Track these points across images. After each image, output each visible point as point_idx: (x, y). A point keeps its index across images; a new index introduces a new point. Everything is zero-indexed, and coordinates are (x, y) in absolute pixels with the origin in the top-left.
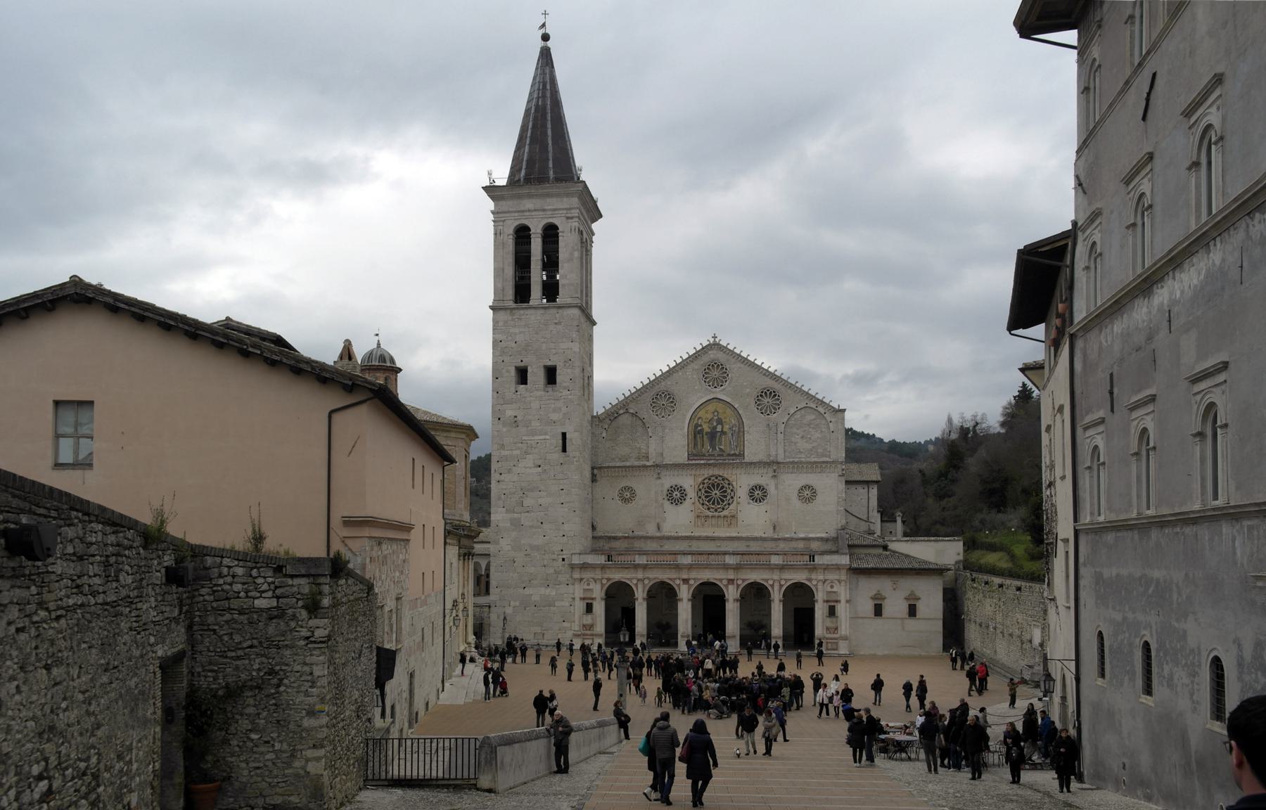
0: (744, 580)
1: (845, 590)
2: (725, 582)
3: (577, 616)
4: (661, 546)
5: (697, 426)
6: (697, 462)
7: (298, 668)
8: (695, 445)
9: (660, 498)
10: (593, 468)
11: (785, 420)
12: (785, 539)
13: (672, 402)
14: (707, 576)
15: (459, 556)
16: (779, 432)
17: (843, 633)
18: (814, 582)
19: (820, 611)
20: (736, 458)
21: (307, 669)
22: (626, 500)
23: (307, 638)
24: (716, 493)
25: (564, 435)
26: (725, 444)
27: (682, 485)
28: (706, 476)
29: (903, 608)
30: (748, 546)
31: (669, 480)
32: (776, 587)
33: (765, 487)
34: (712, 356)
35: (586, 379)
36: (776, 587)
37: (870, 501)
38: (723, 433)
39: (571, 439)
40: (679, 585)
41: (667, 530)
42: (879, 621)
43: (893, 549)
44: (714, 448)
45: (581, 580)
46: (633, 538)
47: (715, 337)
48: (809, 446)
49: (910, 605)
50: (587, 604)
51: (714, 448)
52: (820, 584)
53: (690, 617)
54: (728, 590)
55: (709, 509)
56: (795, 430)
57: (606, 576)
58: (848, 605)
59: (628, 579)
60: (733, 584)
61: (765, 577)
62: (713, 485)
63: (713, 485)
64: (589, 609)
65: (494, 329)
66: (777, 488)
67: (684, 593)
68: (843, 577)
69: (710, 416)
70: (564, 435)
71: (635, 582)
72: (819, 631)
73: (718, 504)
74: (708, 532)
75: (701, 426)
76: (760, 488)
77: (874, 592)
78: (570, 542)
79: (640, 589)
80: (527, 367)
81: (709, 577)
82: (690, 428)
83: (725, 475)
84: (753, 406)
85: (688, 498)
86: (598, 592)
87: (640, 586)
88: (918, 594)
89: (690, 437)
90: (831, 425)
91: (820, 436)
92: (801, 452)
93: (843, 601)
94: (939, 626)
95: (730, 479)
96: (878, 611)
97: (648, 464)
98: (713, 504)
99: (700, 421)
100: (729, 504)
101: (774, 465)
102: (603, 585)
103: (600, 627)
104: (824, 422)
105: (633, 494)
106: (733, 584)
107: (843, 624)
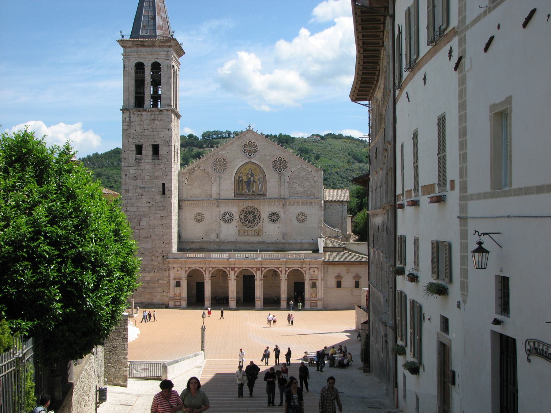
0: (265, 268)
1: (321, 274)
2: (255, 269)
4: (219, 247)
5: (239, 177)
8: (239, 188)
9: (218, 219)
11: (289, 175)
17: (320, 297)
19: (307, 287)
20: (263, 196)
21: (123, 346)
23: (123, 337)
24: (250, 217)
25: (163, 184)
26: (256, 188)
27: (231, 211)
28: (245, 206)
29: (352, 283)
32: (283, 272)
33: (278, 213)
34: (248, 137)
35: (176, 150)
36: (283, 272)
37: (343, 213)
38: (254, 181)
40: (229, 271)
42: (339, 290)
43: (349, 248)
44: (249, 191)
45: (174, 268)
47: (250, 126)
48: (302, 190)
49: (355, 281)
50: (177, 281)
51: (249, 191)
53: (235, 289)
55: (246, 226)
56: (295, 181)
58: (322, 281)
60: (259, 270)
62: (249, 212)
63: (249, 212)
64: (178, 284)
65: (123, 123)
66: (285, 214)
67: (232, 276)
69: (247, 172)
70: (163, 184)
71: (204, 269)
72: (307, 295)
73: (252, 222)
74: (246, 239)
75: (242, 177)
76: (275, 213)
78: (167, 246)
81: (246, 266)
82: (236, 179)
84: (271, 167)
85: (234, 220)
86: (183, 275)
87: (207, 272)
88: (360, 275)
89: (236, 184)
90: (315, 178)
92: (298, 193)
95: (258, 208)
96: (339, 285)
99: (241, 175)
100: (258, 223)
102: (186, 271)
103: (185, 294)
104: (311, 176)
107: (320, 292)
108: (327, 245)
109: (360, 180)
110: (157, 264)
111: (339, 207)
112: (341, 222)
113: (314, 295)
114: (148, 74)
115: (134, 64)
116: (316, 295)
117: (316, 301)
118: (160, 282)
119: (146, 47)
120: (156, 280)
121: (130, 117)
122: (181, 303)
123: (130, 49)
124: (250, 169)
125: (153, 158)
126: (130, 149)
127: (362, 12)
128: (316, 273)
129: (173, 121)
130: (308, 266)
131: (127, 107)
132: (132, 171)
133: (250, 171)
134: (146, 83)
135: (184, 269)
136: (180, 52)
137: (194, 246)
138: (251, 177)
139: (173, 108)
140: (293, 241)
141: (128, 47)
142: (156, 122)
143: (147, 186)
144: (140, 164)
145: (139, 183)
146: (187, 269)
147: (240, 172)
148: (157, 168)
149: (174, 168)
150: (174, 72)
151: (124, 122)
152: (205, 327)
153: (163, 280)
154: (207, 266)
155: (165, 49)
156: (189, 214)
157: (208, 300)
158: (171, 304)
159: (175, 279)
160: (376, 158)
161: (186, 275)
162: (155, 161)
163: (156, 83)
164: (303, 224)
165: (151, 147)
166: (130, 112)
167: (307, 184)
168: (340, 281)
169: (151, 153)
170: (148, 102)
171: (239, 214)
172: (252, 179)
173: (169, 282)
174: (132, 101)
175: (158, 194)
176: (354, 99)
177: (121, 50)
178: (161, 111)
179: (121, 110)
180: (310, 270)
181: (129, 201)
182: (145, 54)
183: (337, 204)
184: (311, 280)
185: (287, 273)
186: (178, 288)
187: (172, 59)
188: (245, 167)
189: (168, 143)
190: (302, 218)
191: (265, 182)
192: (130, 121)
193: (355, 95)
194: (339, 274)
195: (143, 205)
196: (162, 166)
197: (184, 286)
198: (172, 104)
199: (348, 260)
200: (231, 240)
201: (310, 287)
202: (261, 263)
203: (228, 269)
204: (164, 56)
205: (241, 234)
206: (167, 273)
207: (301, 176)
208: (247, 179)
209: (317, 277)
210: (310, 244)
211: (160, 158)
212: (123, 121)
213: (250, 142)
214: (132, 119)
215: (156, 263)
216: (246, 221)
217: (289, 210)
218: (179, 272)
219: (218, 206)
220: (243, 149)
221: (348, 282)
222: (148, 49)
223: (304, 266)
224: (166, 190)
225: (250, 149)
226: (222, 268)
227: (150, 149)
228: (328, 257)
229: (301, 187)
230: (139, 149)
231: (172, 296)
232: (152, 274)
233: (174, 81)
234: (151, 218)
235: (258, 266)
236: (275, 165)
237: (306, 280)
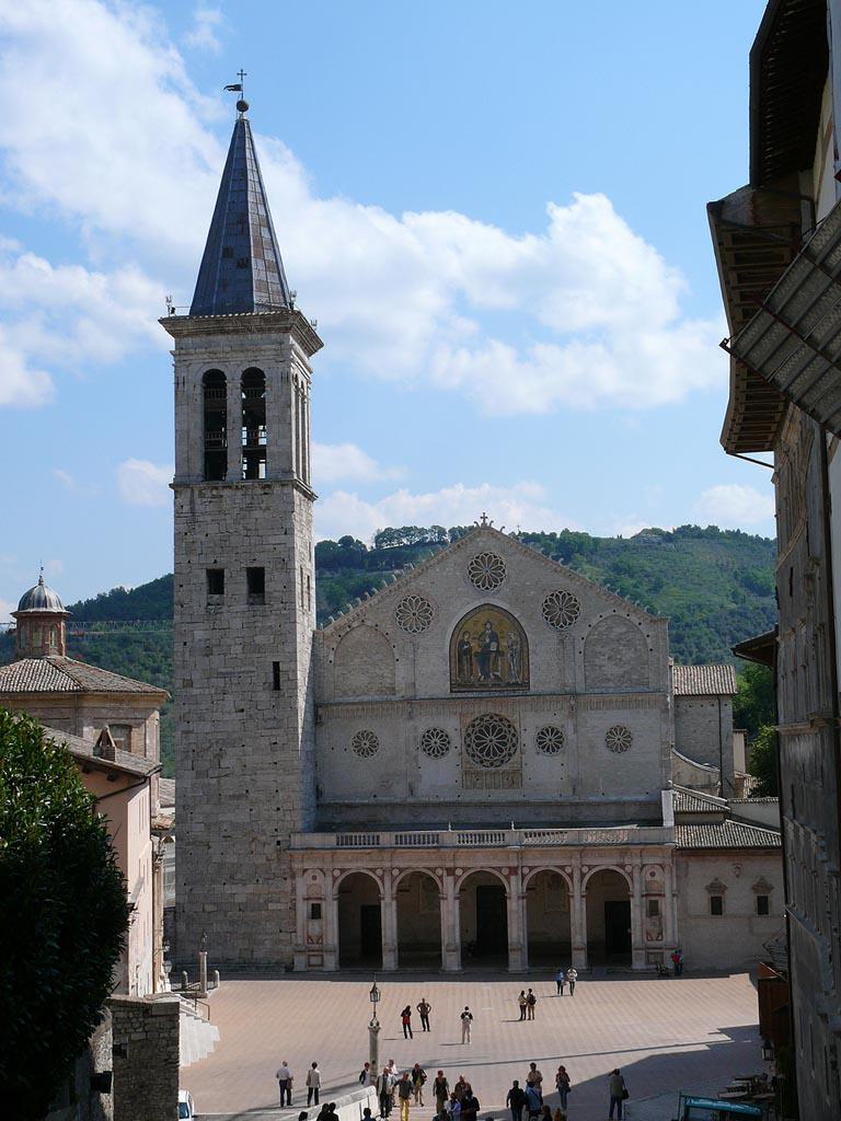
0: (531, 868)
1: (671, 878)
2: (505, 872)
5: (462, 643)
6: (464, 695)
7: (160, 1081)
8: (461, 670)
12: (590, 804)
13: (427, 611)
14: (481, 862)
16: (577, 653)
19: (637, 913)
22: (364, 752)
23: (166, 1060)
24: (491, 740)
25: (276, 665)
27: (443, 727)
28: (477, 715)
30: (537, 814)
32: (576, 876)
35: (305, 581)
36: (576, 876)
40: (441, 877)
41: (424, 792)
42: (718, 922)
44: (487, 675)
45: (305, 871)
46: (375, 806)
47: (484, 518)
48: (618, 671)
51: (487, 675)
52: (636, 871)
54: (509, 883)
55: (482, 762)
56: (598, 649)
58: (675, 898)
59: (371, 870)
60: (516, 874)
62: (487, 728)
63: (487, 728)
64: (316, 913)
66: (576, 731)
67: (449, 888)
68: (668, 861)
70: (276, 665)
71: (379, 872)
72: (636, 937)
73: (495, 754)
79: (388, 884)
80: (223, 571)
81: (482, 864)
82: (453, 647)
85: (452, 749)
86: (328, 888)
89: (453, 660)
90: (649, 640)
93: (668, 895)
95: (509, 719)
96: (717, 907)
97: (394, 698)
98: (488, 755)
99: (466, 637)
100: (510, 755)
101: (571, 697)
102: (335, 878)
103: (332, 938)
104: (638, 636)
106: (516, 874)
107: (669, 925)
108: (685, 809)
110: (264, 861)
111: (710, 709)
113: (654, 936)
114: (235, 397)
118: (271, 906)
119: (228, 332)
120: (262, 901)
121: (192, 502)
122: (323, 958)
123: (190, 340)
125: (251, 601)
127: (736, 239)
128: (657, 878)
129: (297, 509)
130: (638, 861)
132: (199, 634)
133: (488, 626)
134: (230, 419)
135: (329, 874)
136: (312, 343)
137: (352, 816)
138: (490, 642)
141: (188, 335)
142: (257, 514)
144: (218, 616)
145: (216, 661)
146: (337, 873)
147: (463, 631)
148: (260, 625)
149: (303, 624)
151: (178, 515)
152: (378, 1024)
154: (387, 864)
155: (274, 336)
156: (340, 736)
157: (390, 951)
158: (300, 962)
159: (308, 899)
160: (791, 594)
161: (336, 891)
162: (257, 607)
163: (255, 416)
164: (622, 757)
166: (193, 491)
167: (629, 655)
168: (720, 898)
169: (244, 588)
170: (237, 466)
171: (464, 734)
172: (493, 647)
173: (293, 908)
174: (198, 465)
175: (264, 689)
176: (732, 447)
178: (269, 486)
181: (193, 707)
182: (227, 349)
183: (706, 703)
184: (646, 895)
185: (587, 877)
186: (316, 922)
187: (292, 360)
188: (474, 619)
189: (286, 563)
190: (620, 740)
191: (525, 654)
192: (193, 511)
193: (734, 438)
194: (716, 879)
195: (227, 717)
196: (271, 621)
197: (330, 918)
199: (739, 844)
201: (644, 915)
202: (520, 854)
204: (274, 353)
205: (469, 784)
206: (287, 886)
207: (612, 636)
208: (480, 646)
209: (662, 886)
211: (267, 601)
212: (176, 512)
213: (486, 555)
214: (199, 508)
215: (261, 860)
217: (586, 722)
219: (410, 717)
220: (470, 572)
221: (739, 899)
223: (627, 861)
225: (486, 571)
226: (424, 871)
227: (243, 578)
228: (685, 837)
229: (616, 664)
230: (216, 580)
232: (251, 888)
233: (297, 413)
234: (248, 749)
235: (514, 864)
236: (548, 610)
237: (633, 896)
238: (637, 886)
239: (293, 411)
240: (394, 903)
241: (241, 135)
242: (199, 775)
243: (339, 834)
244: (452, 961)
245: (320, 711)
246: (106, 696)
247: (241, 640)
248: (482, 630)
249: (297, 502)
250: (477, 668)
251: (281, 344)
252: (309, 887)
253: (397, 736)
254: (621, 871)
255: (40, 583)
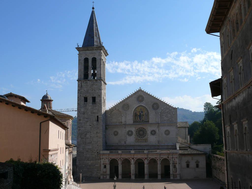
0: (150, 158)
1: (179, 160)
2: (144, 159)
3: (102, 169)
5: (135, 113)
8: (135, 118)
10: (106, 126)
12: (162, 146)
14: (139, 156)
15: (69, 154)
16: (159, 115)
18: (170, 158)
22: (115, 135)
24: (141, 133)
25: (98, 116)
28: (138, 127)
31: (128, 129)
32: (159, 160)
35: (104, 100)
38: (143, 115)
39: (100, 118)
40: (131, 160)
41: (128, 143)
44: (141, 120)
47: (140, 88)
50: (105, 165)
51: (141, 120)
55: (139, 137)
57: (110, 157)
58: (179, 165)
60: (146, 159)
61: (156, 157)
64: (105, 167)
66: (159, 131)
69: (139, 110)
70: (98, 116)
71: (118, 159)
72: (171, 172)
74: (139, 144)
75: (137, 113)
77: (187, 161)
78: (100, 147)
81: (139, 157)
83: (144, 127)
85: (133, 134)
86: (107, 162)
89: (134, 116)
90: (173, 113)
91: (170, 116)
94: (205, 170)
96: (188, 166)
97: (122, 124)
98: (141, 135)
99: (136, 112)
101: (158, 124)
102: (109, 160)
103: (108, 172)
105: (118, 133)
108: (181, 146)
109: (216, 83)
111: (183, 130)
112: (185, 137)
115: (84, 58)
116: (176, 172)
117: (176, 175)
118: (96, 165)
119: (89, 50)
120: (94, 164)
121: (81, 84)
123: (81, 52)
124: (141, 109)
125: (93, 103)
126: (82, 99)
128: (176, 160)
129: (102, 85)
130: (171, 157)
131: (80, 79)
132: (82, 110)
134: (89, 67)
135: (108, 159)
136: (106, 54)
138: (141, 113)
139: (102, 79)
140: (163, 144)
141: (81, 51)
142: (94, 86)
143: (90, 117)
144: (86, 106)
146: (110, 159)
147: (136, 110)
149: (103, 108)
150: (103, 62)
151: (78, 86)
152: (116, 185)
153: (98, 165)
154: (120, 157)
155: (98, 51)
158: (102, 177)
159: (104, 164)
161: (109, 162)
162: (94, 105)
163: (94, 68)
165: (91, 98)
166: (81, 82)
167: (169, 115)
168: (188, 164)
169: (91, 101)
172: (142, 114)
173: (101, 166)
174: (83, 77)
177: (78, 52)
178: (97, 80)
179: (77, 80)
180: (173, 158)
183: (183, 129)
184: (174, 164)
185: (161, 160)
186: (105, 169)
187: (102, 56)
190: (167, 133)
194: (188, 160)
195: (87, 127)
198: (102, 77)
199: (192, 153)
200: (132, 145)
201: (173, 167)
202: (148, 154)
203: (131, 159)
207: (166, 112)
209: (177, 162)
210: (172, 146)
212: (78, 86)
214: (83, 85)
215: (94, 156)
216: (139, 135)
218: (106, 160)
219: (125, 128)
221: (193, 164)
222: (90, 51)
224: (99, 119)
225: (140, 98)
227: (91, 99)
228: (181, 152)
231: (102, 173)
232: (92, 162)
234: (92, 133)
235: (146, 157)
238: (171, 161)
239: (102, 66)
240: (121, 165)
241: (93, 13)
242: (82, 138)
243: (110, 151)
244: (133, 177)
245: (107, 127)
246: (59, 116)
247: (90, 111)
248: (140, 110)
249: (102, 84)
250: (138, 118)
251: (100, 52)
252: (104, 161)
253: (122, 132)
254: (168, 159)
255: (47, 94)
